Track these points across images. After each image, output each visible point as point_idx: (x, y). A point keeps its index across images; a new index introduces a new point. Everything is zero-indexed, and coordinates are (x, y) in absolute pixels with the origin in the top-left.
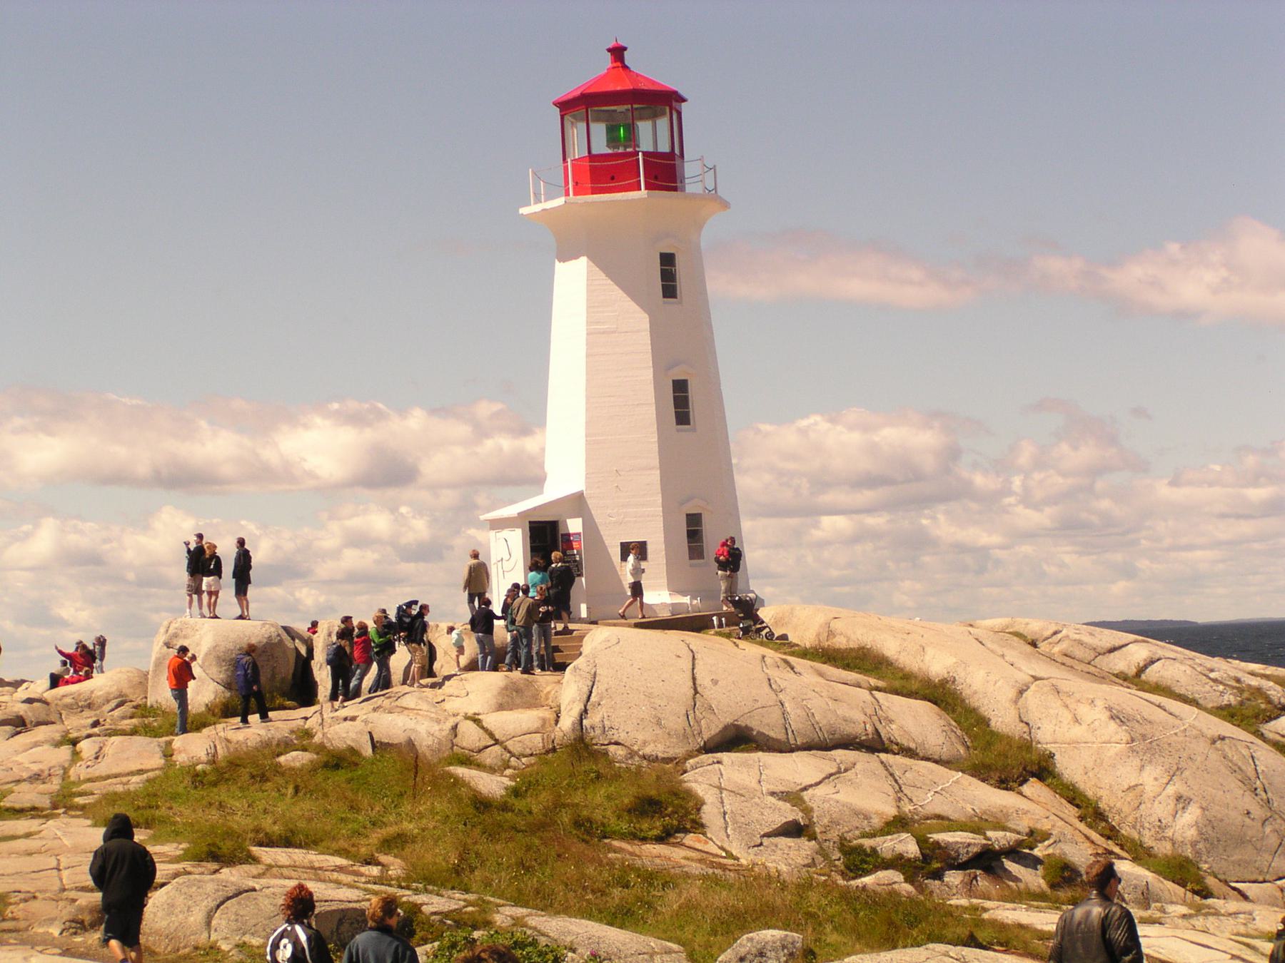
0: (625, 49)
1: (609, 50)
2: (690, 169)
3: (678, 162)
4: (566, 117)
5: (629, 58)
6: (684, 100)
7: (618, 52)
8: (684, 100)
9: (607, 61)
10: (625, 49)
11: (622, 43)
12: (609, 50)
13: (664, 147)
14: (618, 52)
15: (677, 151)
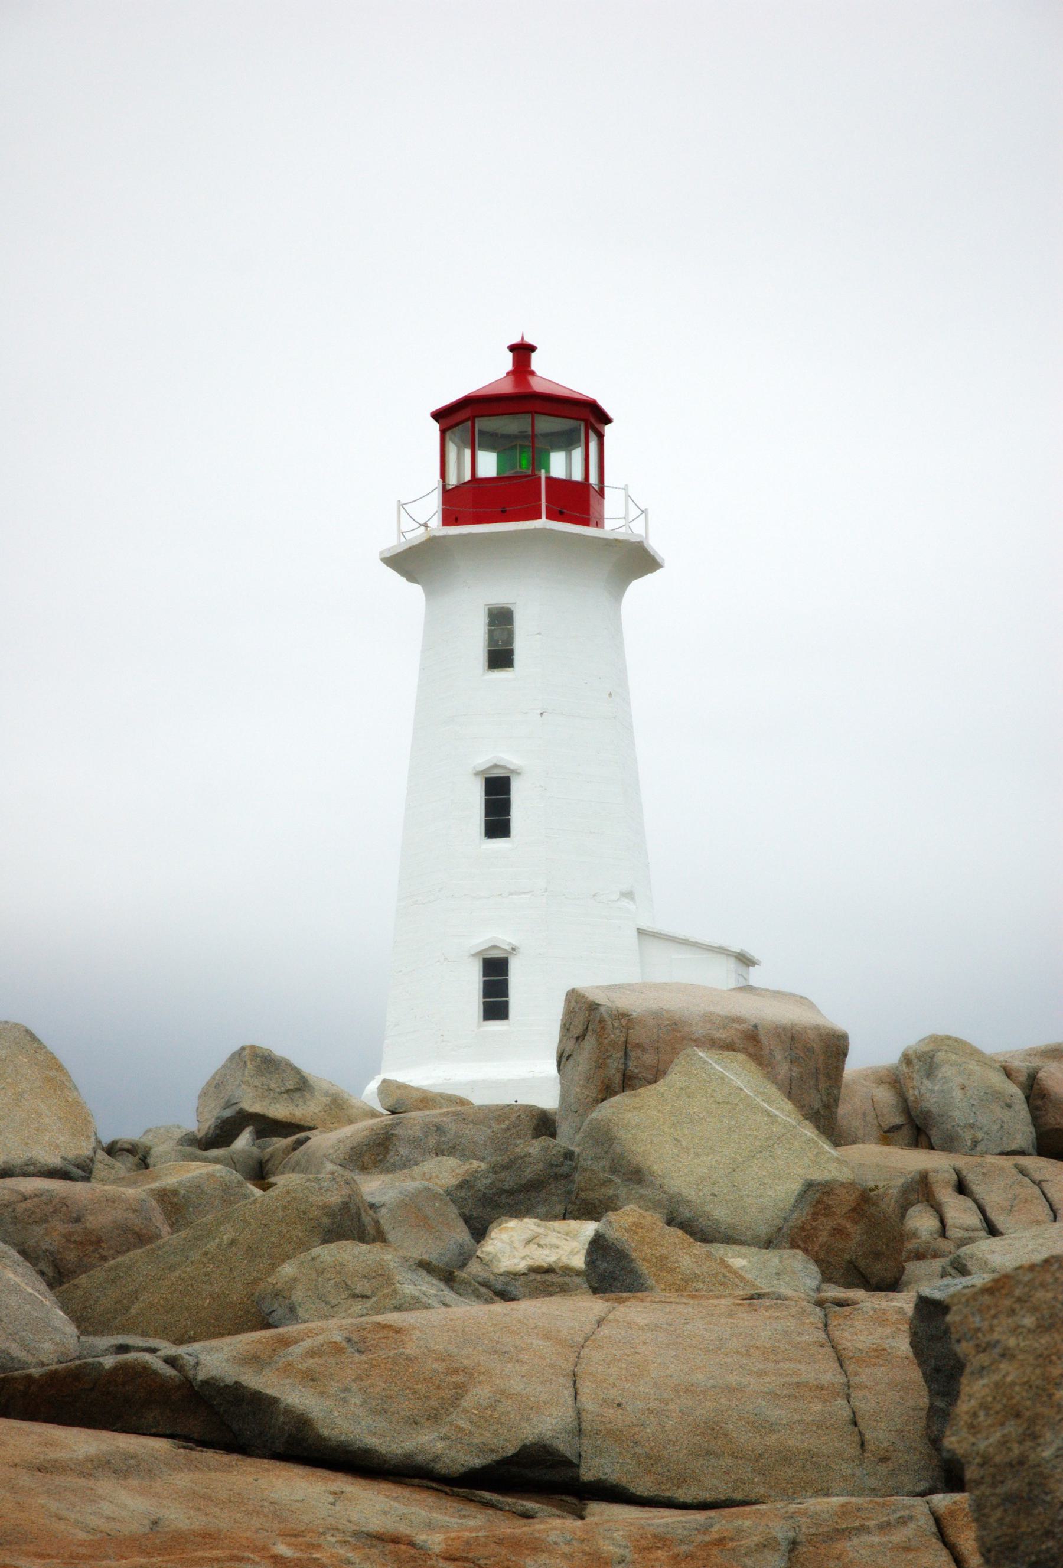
0: (533, 349)
1: (512, 348)
2: (613, 506)
3: (593, 497)
4: (448, 435)
5: (537, 362)
6: (607, 420)
7: (522, 352)
8: (607, 420)
9: (506, 362)
10: (533, 349)
11: (529, 340)
12: (512, 348)
13: (577, 476)
14: (522, 352)
15: (593, 479)
